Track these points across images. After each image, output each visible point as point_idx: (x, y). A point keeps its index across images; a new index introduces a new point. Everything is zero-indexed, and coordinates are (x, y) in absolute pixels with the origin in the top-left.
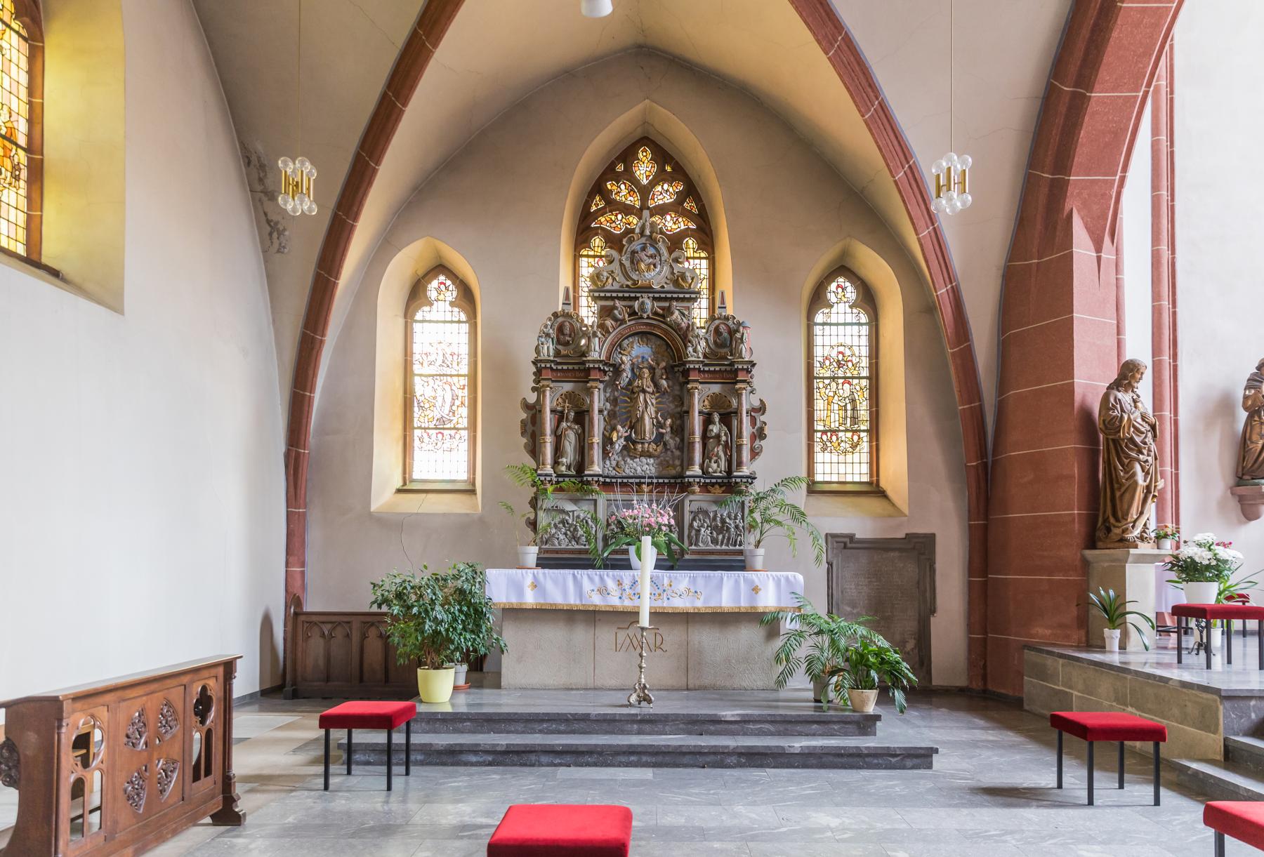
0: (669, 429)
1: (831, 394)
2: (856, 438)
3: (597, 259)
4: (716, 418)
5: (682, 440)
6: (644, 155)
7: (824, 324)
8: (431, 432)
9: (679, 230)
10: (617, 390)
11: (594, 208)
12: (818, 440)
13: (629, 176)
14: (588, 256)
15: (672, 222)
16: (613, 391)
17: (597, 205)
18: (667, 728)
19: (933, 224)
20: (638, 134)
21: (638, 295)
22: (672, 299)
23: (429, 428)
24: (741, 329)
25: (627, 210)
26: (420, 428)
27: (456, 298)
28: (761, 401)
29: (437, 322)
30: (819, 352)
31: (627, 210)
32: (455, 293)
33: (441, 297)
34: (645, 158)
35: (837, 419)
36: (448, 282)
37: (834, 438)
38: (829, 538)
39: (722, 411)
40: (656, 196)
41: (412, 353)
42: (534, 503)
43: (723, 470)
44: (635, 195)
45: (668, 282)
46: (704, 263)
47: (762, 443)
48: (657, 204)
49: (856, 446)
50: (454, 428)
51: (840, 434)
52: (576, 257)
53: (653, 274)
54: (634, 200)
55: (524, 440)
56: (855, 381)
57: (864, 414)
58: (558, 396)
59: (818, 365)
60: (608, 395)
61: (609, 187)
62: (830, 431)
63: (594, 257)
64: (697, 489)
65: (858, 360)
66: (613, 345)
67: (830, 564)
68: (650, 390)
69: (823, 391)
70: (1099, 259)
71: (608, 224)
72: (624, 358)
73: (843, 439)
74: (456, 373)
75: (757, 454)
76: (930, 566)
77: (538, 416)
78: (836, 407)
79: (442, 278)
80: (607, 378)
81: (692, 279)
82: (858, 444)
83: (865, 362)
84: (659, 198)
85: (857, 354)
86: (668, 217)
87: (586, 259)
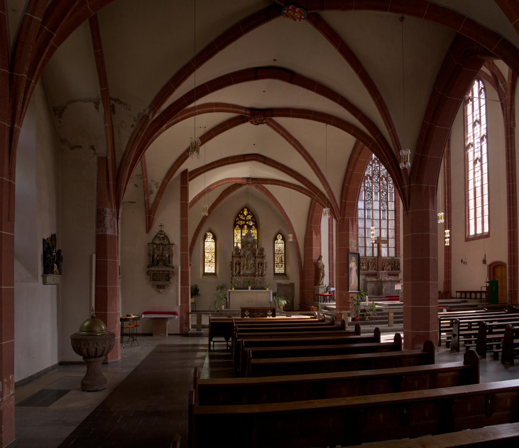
4: (260, 264)
7: (276, 243)
14: (236, 229)
30: (276, 248)
32: (212, 236)
36: (211, 234)
42: (232, 279)
46: (256, 231)
52: (234, 229)
57: (283, 260)
63: (237, 229)
83: (284, 250)
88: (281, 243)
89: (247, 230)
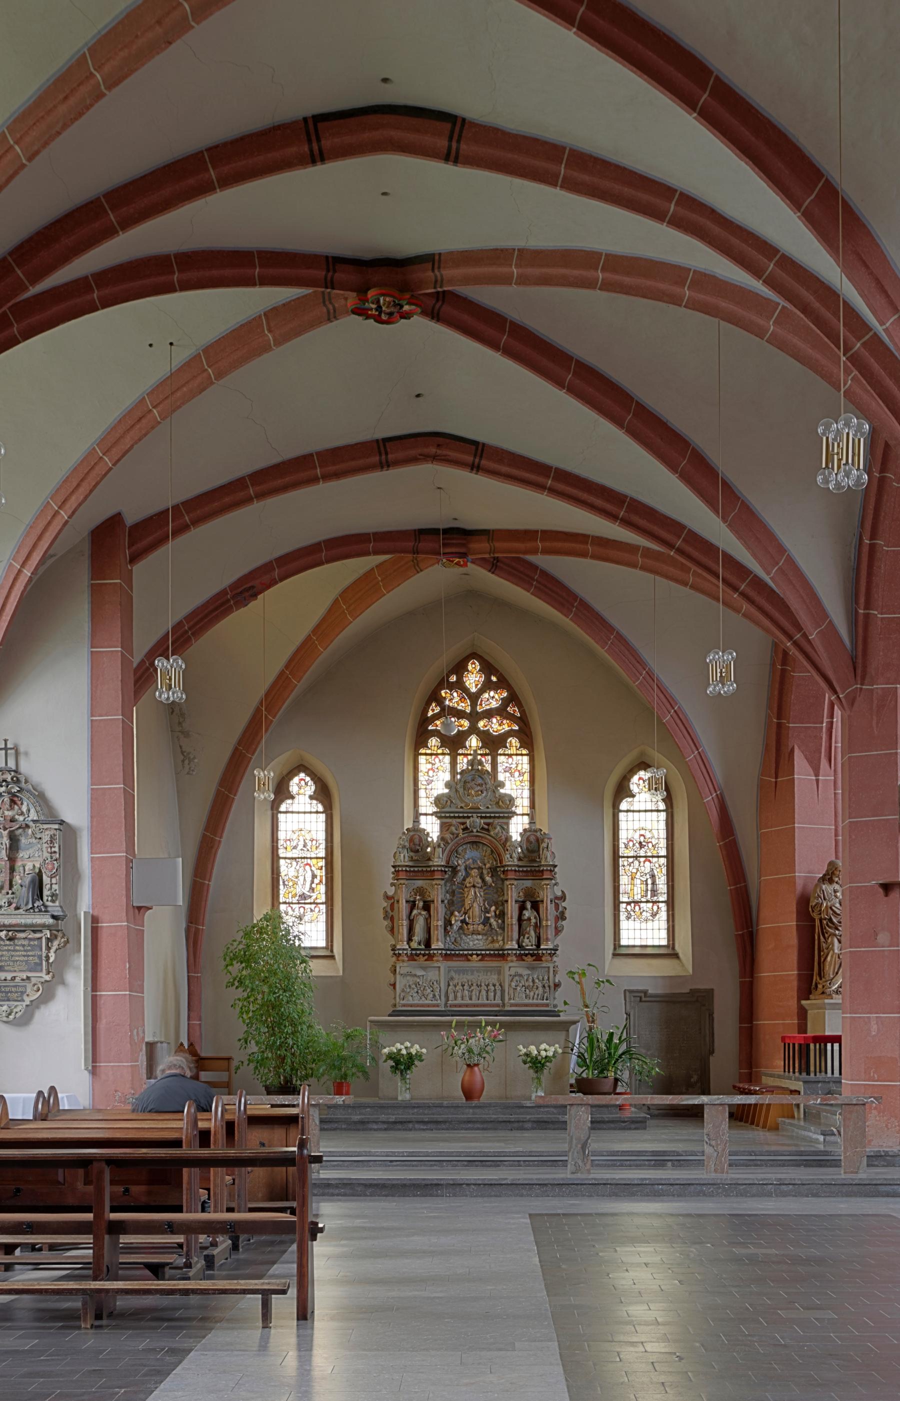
0: (493, 914)
1: (635, 871)
2: (655, 908)
3: (433, 757)
4: (529, 905)
5: (504, 922)
6: (474, 666)
7: (627, 811)
8: (294, 906)
10: (455, 885)
11: (430, 713)
12: (624, 910)
13: (460, 685)
14: (426, 754)
16: (451, 885)
17: (433, 710)
18: (491, 1112)
19: (698, 750)
20: (469, 652)
21: (470, 815)
22: (495, 817)
23: (292, 903)
24: (546, 840)
25: (460, 714)
26: (285, 903)
27: (315, 792)
28: (562, 892)
30: (623, 836)
31: (460, 714)
32: (313, 788)
33: (302, 791)
35: (639, 892)
36: (308, 779)
37: (637, 908)
38: (627, 994)
39: (533, 900)
41: (278, 840)
43: (534, 943)
45: (491, 803)
46: (526, 759)
47: (564, 923)
49: (656, 915)
50: (314, 903)
51: (642, 905)
52: (416, 755)
53: (480, 798)
54: (465, 706)
55: (386, 923)
56: (655, 860)
57: (662, 887)
58: (411, 890)
59: (623, 846)
60: (448, 888)
61: (443, 695)
62: (634, 902)
63: (431, 755)
64: (514, 958)
65: (657, 841)
66: (451, 852)
67: (628, 1015)
68: (480, 885)
69: (627, 868)
70: (817, 781)
72: (460, 862)
73: (645, 909)
74: (315, 856)
75: (560, 931)
76: (709, 1015)
77: (396, 905)
78: (639, 882)
79: (302, 775)
80: (447, 876)
81: (510, 801)
82: (657, 913)
83: (663, 843)
85: (656, 836)
86: (494, 720)
87: (424, 757)
88: (652, 811)
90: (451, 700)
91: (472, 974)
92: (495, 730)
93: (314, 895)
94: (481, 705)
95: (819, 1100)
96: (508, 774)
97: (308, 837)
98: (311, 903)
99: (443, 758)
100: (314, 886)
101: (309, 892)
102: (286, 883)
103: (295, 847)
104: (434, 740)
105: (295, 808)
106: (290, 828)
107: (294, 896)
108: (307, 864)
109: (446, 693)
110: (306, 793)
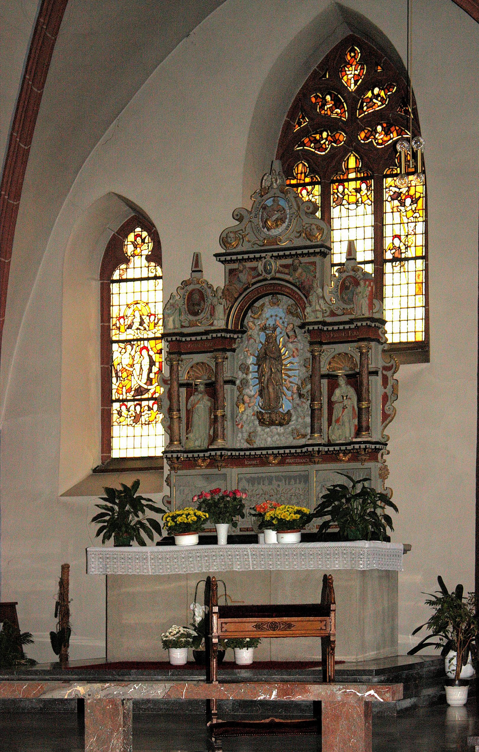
8: (129, 404)
9: (391, 141)
15: (383, 132)
26: (118, 400)
27: (152, 251)
29: (134, 280)
32: (151, 245)
34: (354, 59)
36: (145, 234)
40: (365, 104)
44: (341, 106)
48: (366, 113)
61: (313, 100)
71: (313, 145)
74: (153, 336)
84: (368, 106)
89: (363, 180)
90: (322, 107)
91: (270, 483)
92: (380, 141)
93: (152, 388)
94: (362, 107)
95: (275, 693)
96: (396, 203)
97: (145, 312)
98: (148, 399)
99: (313, 189)
100: (152, 376)
101: (145, 384)
102: (120, 374)
103: (130, 327)
104: (301, 166)
105: (130, 274)
106: (123, 302)
107: (129, 391)
108: (145, 348)
109: (317, 97)
110: (143, 253)
